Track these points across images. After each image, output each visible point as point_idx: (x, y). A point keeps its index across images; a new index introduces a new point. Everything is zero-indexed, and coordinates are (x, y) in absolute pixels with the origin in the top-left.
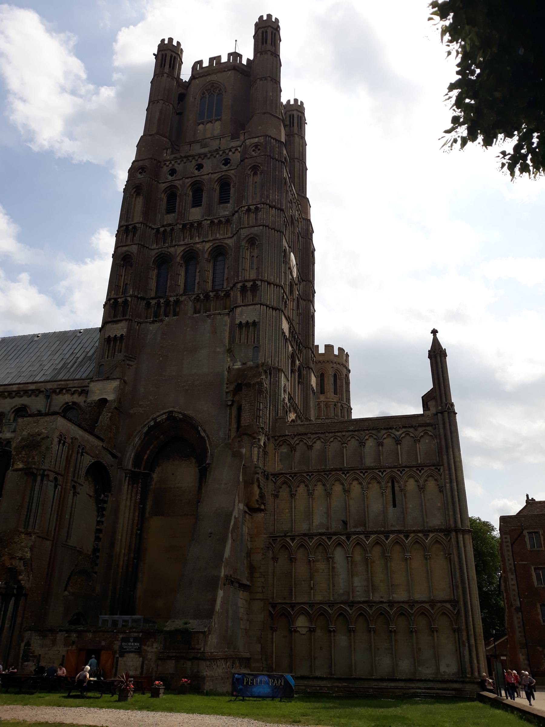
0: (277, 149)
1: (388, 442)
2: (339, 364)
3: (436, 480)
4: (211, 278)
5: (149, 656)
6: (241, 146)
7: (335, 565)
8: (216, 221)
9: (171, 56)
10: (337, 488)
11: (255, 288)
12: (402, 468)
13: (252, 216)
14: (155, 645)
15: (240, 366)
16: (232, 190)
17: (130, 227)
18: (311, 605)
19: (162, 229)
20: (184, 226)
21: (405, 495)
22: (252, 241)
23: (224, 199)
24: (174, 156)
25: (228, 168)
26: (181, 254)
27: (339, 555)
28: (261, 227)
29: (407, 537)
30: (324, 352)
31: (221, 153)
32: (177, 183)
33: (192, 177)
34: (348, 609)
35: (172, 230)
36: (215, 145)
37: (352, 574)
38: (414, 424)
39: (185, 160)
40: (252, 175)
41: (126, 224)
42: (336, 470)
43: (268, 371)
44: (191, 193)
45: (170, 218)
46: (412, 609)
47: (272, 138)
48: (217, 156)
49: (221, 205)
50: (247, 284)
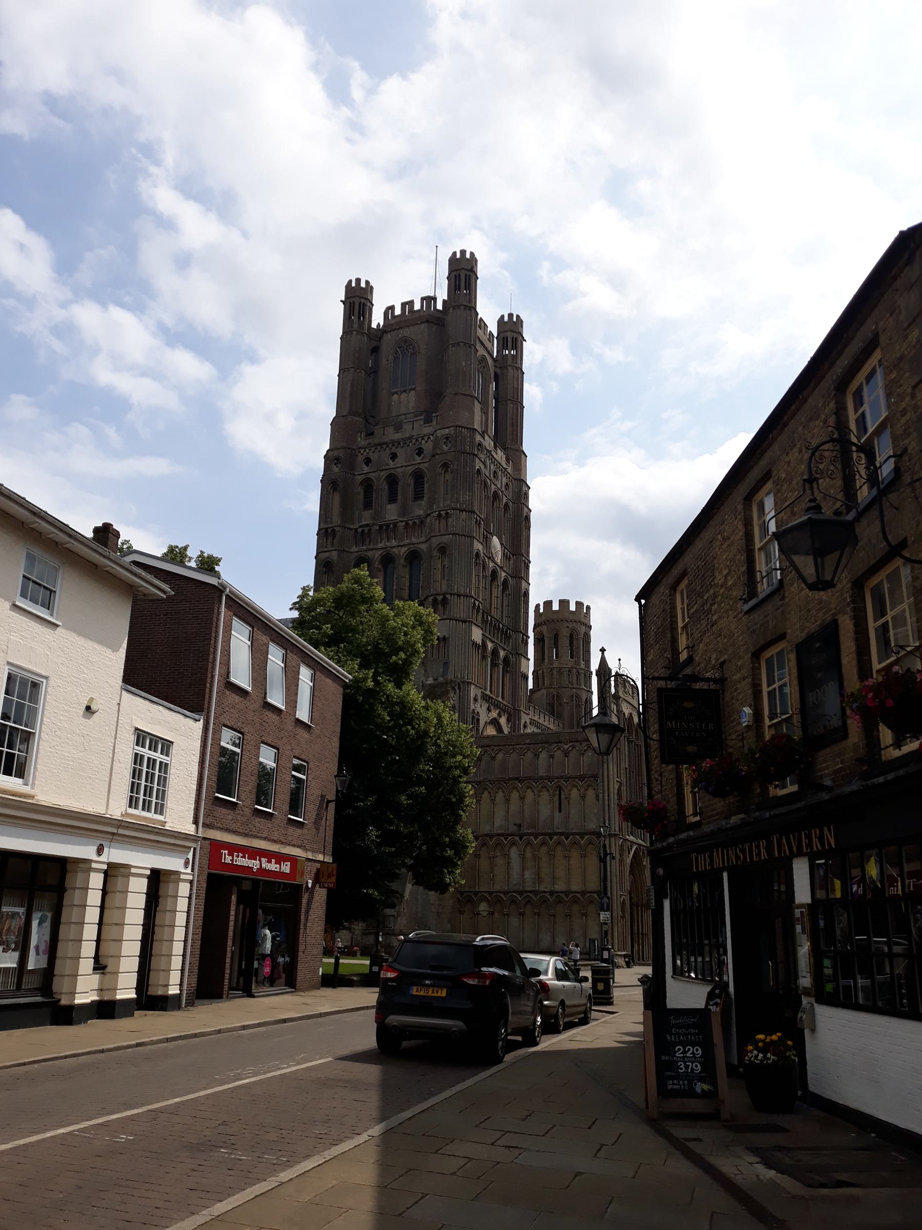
0: (469, 439)
1: (559, 754)
2: (575, 622)
3: (594, 789)
4: (407, 584)
5: (357, 932)
6: (433, 435)
7: (510, 861)
8: (410, 523)
9: (360, 303)
10: (515, 795)
11: (445, 602)
12: (567, 778)
13: (443, 522)
14: (360, 925)
15: (432, 682)
16: (426, 486)
17: (329, 530)
18: (490, 893)
19: (360, 530)
20: (381, 526)
21: (568, 801)
22: (443, 550)
23: (418, 496)
24: (368, 441)
25: (422, 459)
26: (380, 558)
27: (514, 852)
28: (451, 536)
29: (567, 838)
30: (558, 609)
31: (414, 441)
32: (371, 476)
33: (386, 470)
34: (518, 897)
35: (370, 530)
36: (407, 430)
37: (523, 869)
38: (580, 738)
39: (379, 448)
40: (443, 473)
41: (325, 526)
42: (513, 779)
43: (456, 688)
44: (386, 487)
45: (366, 517)
46: (567, 898)
47: (462, 427)
48: (411, 444)
49: (416, 503)
50: (438, 597)
